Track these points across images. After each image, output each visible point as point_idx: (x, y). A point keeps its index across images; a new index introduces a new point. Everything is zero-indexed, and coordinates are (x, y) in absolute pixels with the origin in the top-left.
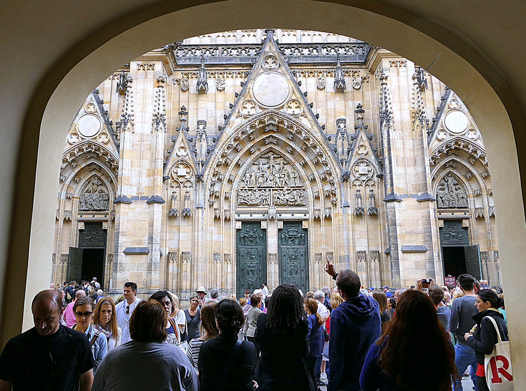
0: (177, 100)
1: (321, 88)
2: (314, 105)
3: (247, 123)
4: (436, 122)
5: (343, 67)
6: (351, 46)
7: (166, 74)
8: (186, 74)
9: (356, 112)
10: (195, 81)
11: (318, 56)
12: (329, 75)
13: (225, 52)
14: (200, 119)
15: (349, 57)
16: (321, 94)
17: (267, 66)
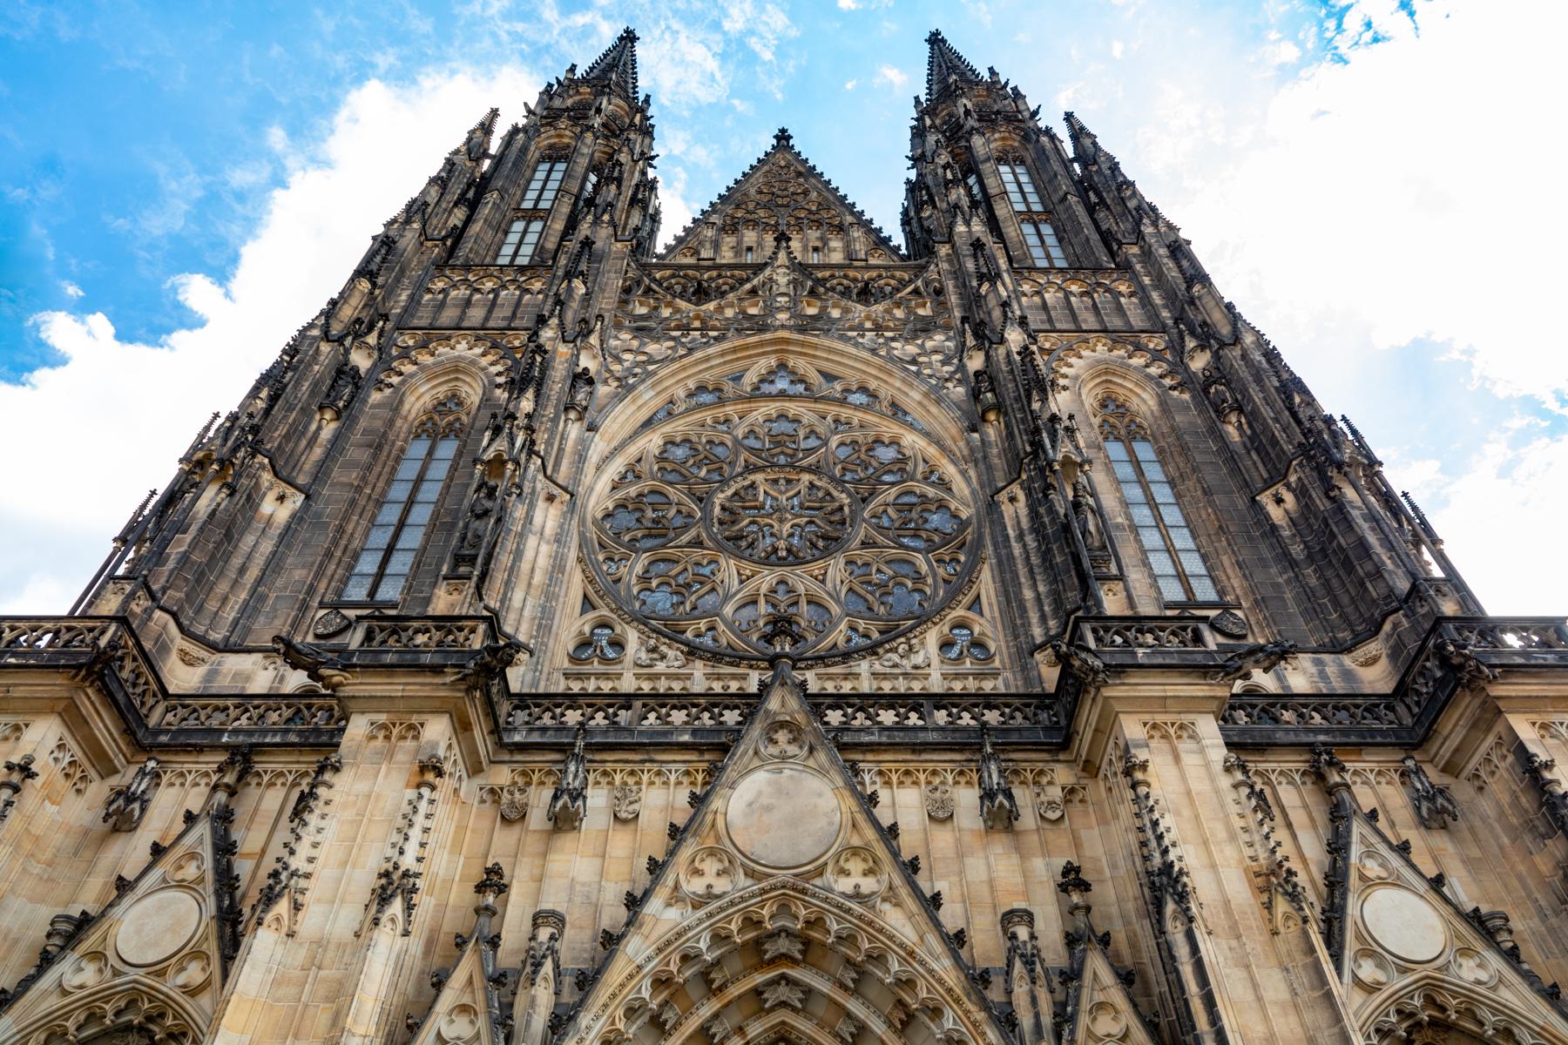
0: (482, 849)
1: (941, 816)
2: (923, 864)
3: (701, 921)
4: (1336, 924)
5: (1002, 757)
6: (1017, 702)
7: (461, 765)
8: (524, 774)
9: (1064, 888)
10: (548, 793)
11: (923, 729)
12: (963, 780)
13: (652, 716)
14: (547, 905)
15: (1018, 730)
16: (943, 838)
17: (773, 750)
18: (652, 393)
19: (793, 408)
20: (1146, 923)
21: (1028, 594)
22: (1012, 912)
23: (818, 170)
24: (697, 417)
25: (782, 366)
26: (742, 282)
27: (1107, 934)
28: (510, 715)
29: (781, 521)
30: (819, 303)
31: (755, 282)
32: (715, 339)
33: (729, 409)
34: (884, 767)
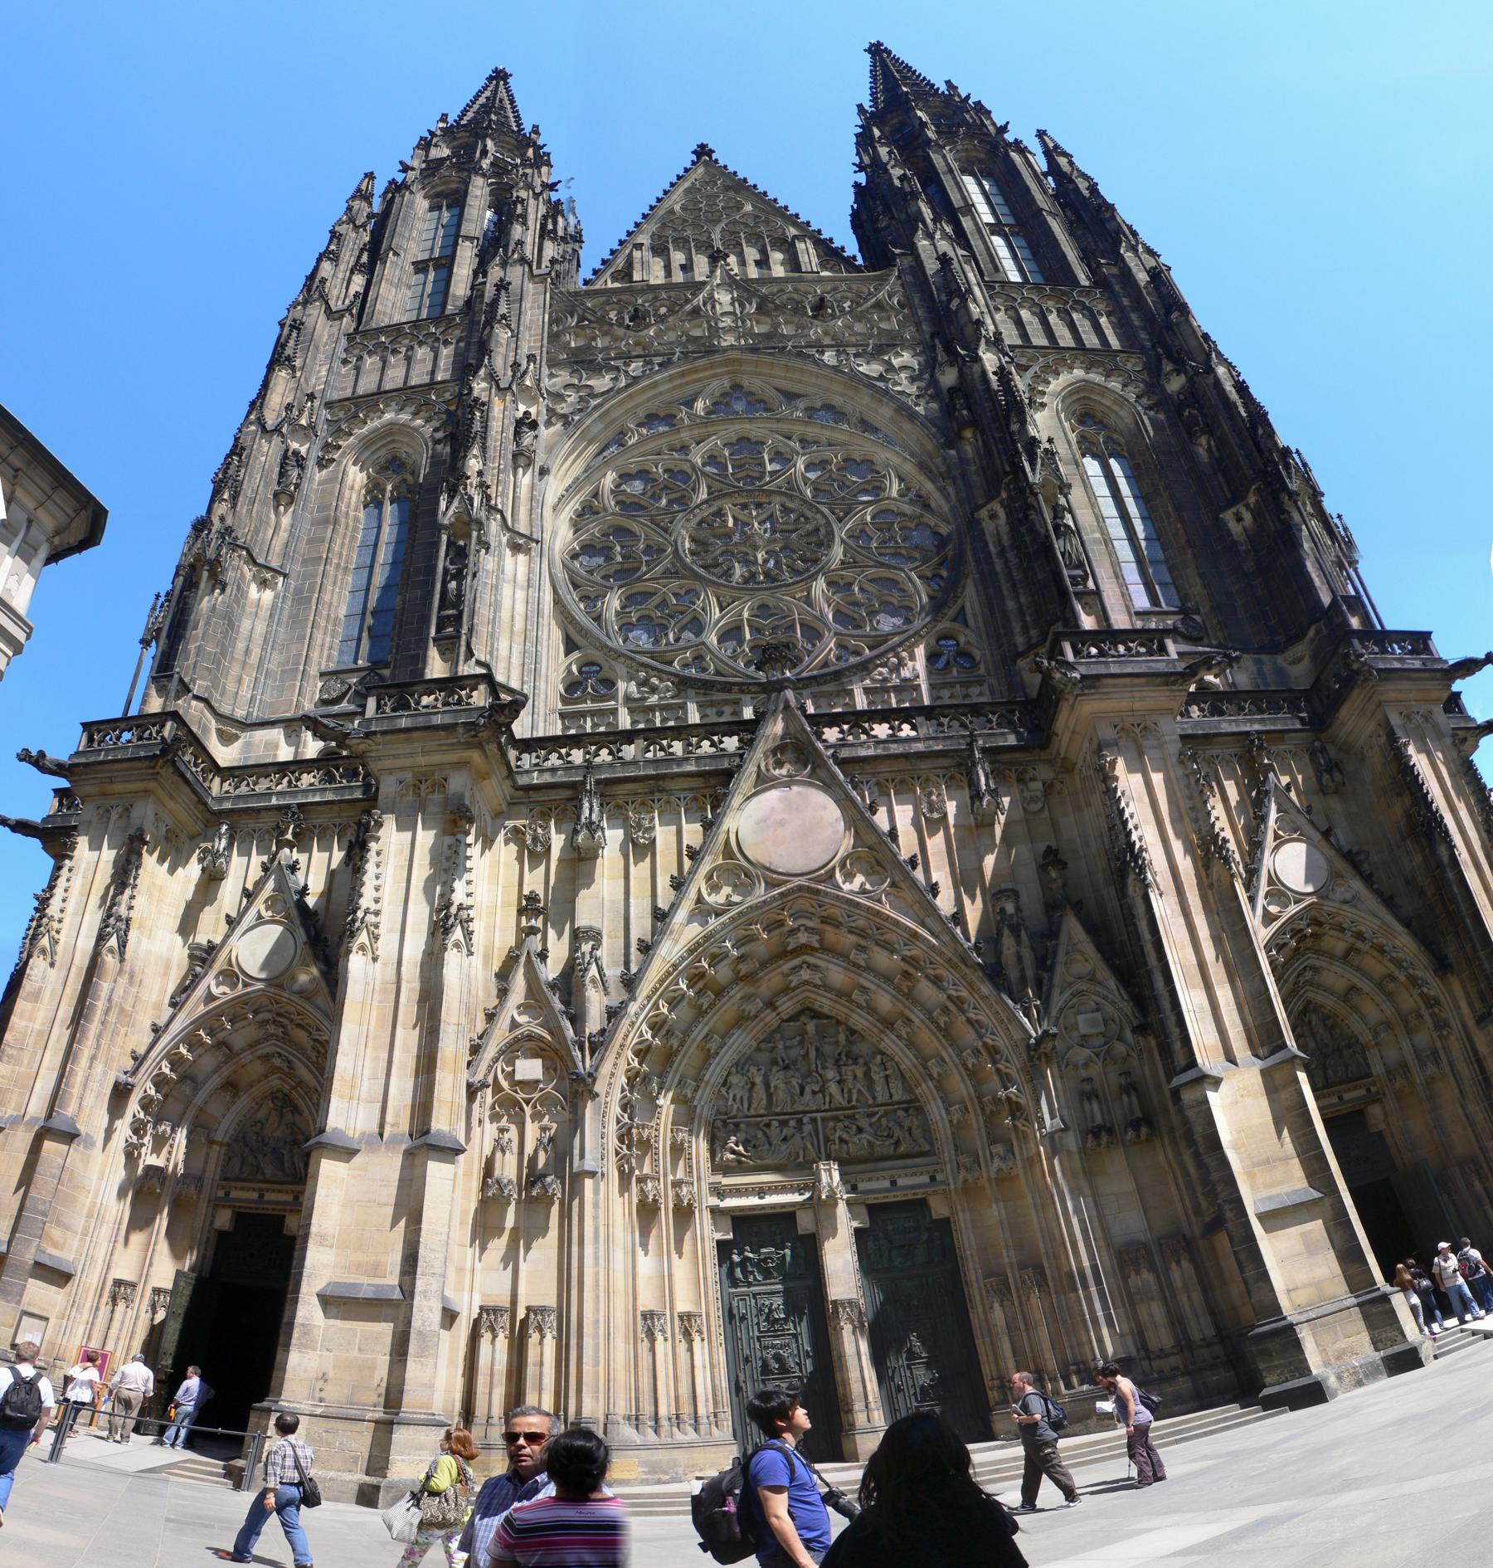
18: (600, 426)
19: (754, 430)
20: (1112, 889)
21: (1011, 605)
22: (1001, 892)
23: (751, 182)
24: (651, 446)
25: (736, 387)
26: (682, 306)
27: (1080, 902)
28: (518, 759)
29: (756, 548)
30: (768, 320)
31: (695, 302)
32: (660, 365)
33: (685, 435)
34: (881, 778)
